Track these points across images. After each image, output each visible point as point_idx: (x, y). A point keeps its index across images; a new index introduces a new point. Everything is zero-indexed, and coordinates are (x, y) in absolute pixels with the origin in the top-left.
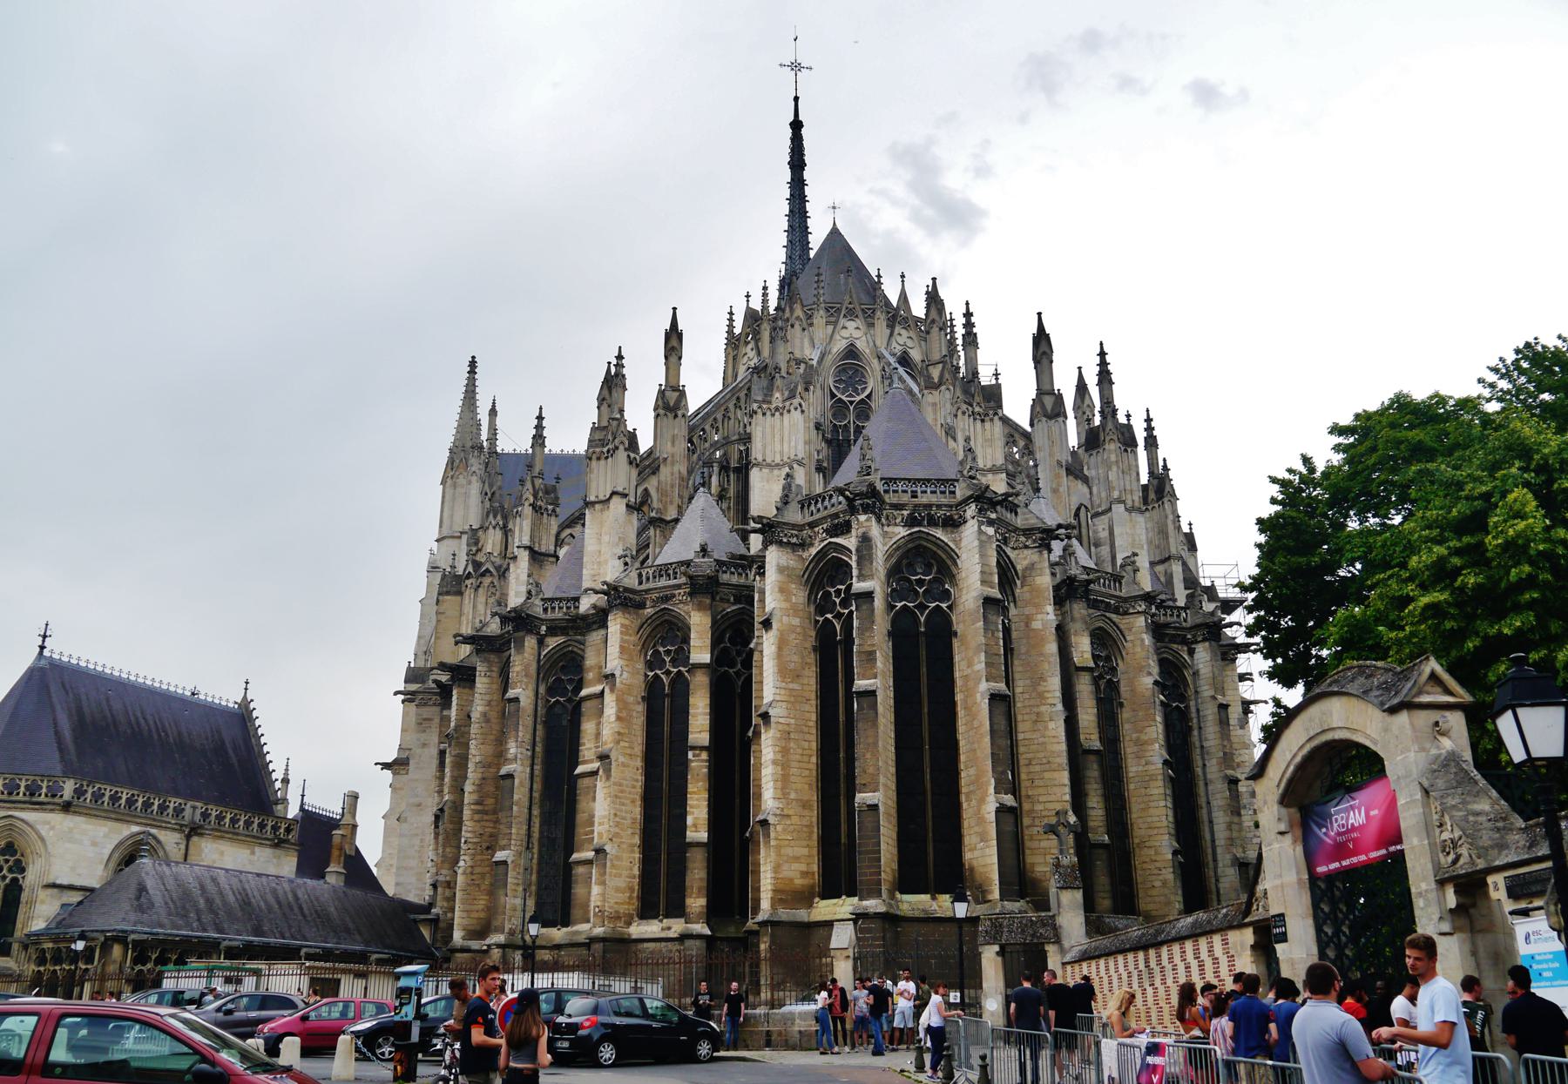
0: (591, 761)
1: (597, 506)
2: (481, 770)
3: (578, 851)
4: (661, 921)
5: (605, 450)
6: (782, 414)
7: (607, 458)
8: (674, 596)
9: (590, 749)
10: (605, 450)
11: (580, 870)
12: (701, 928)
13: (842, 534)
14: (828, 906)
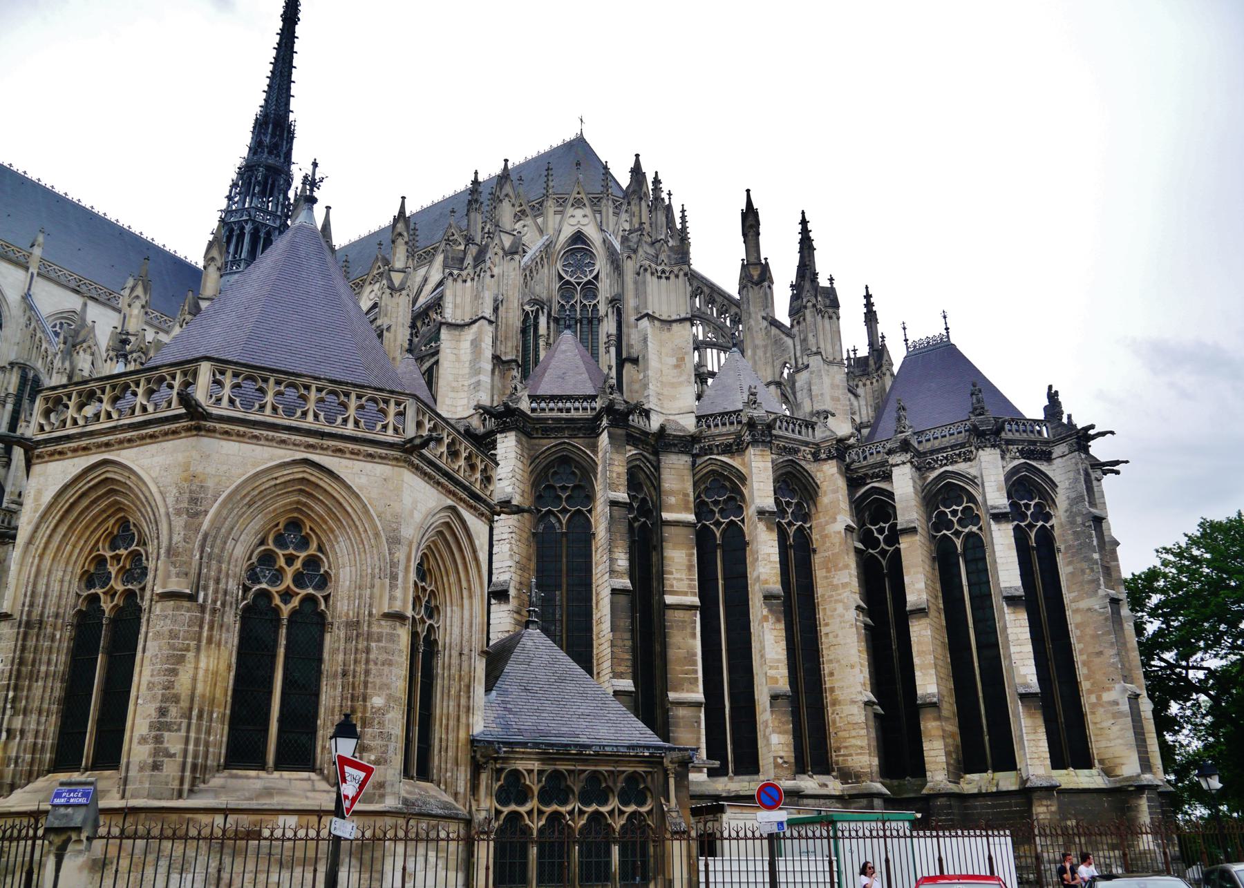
0: (685, 594)
1: (656, 322)
2: (519, 572)
3: (675, 690)
4: (811, 777)
5: (659, 268)
6: (823, 317)
7: (659, 277)
8: (799, 451)
9: (682, 580)
10: (659, 268)
11: (682, 712)
12: (878, 787)
13: (1034, 459)
14: (1061, 776)
